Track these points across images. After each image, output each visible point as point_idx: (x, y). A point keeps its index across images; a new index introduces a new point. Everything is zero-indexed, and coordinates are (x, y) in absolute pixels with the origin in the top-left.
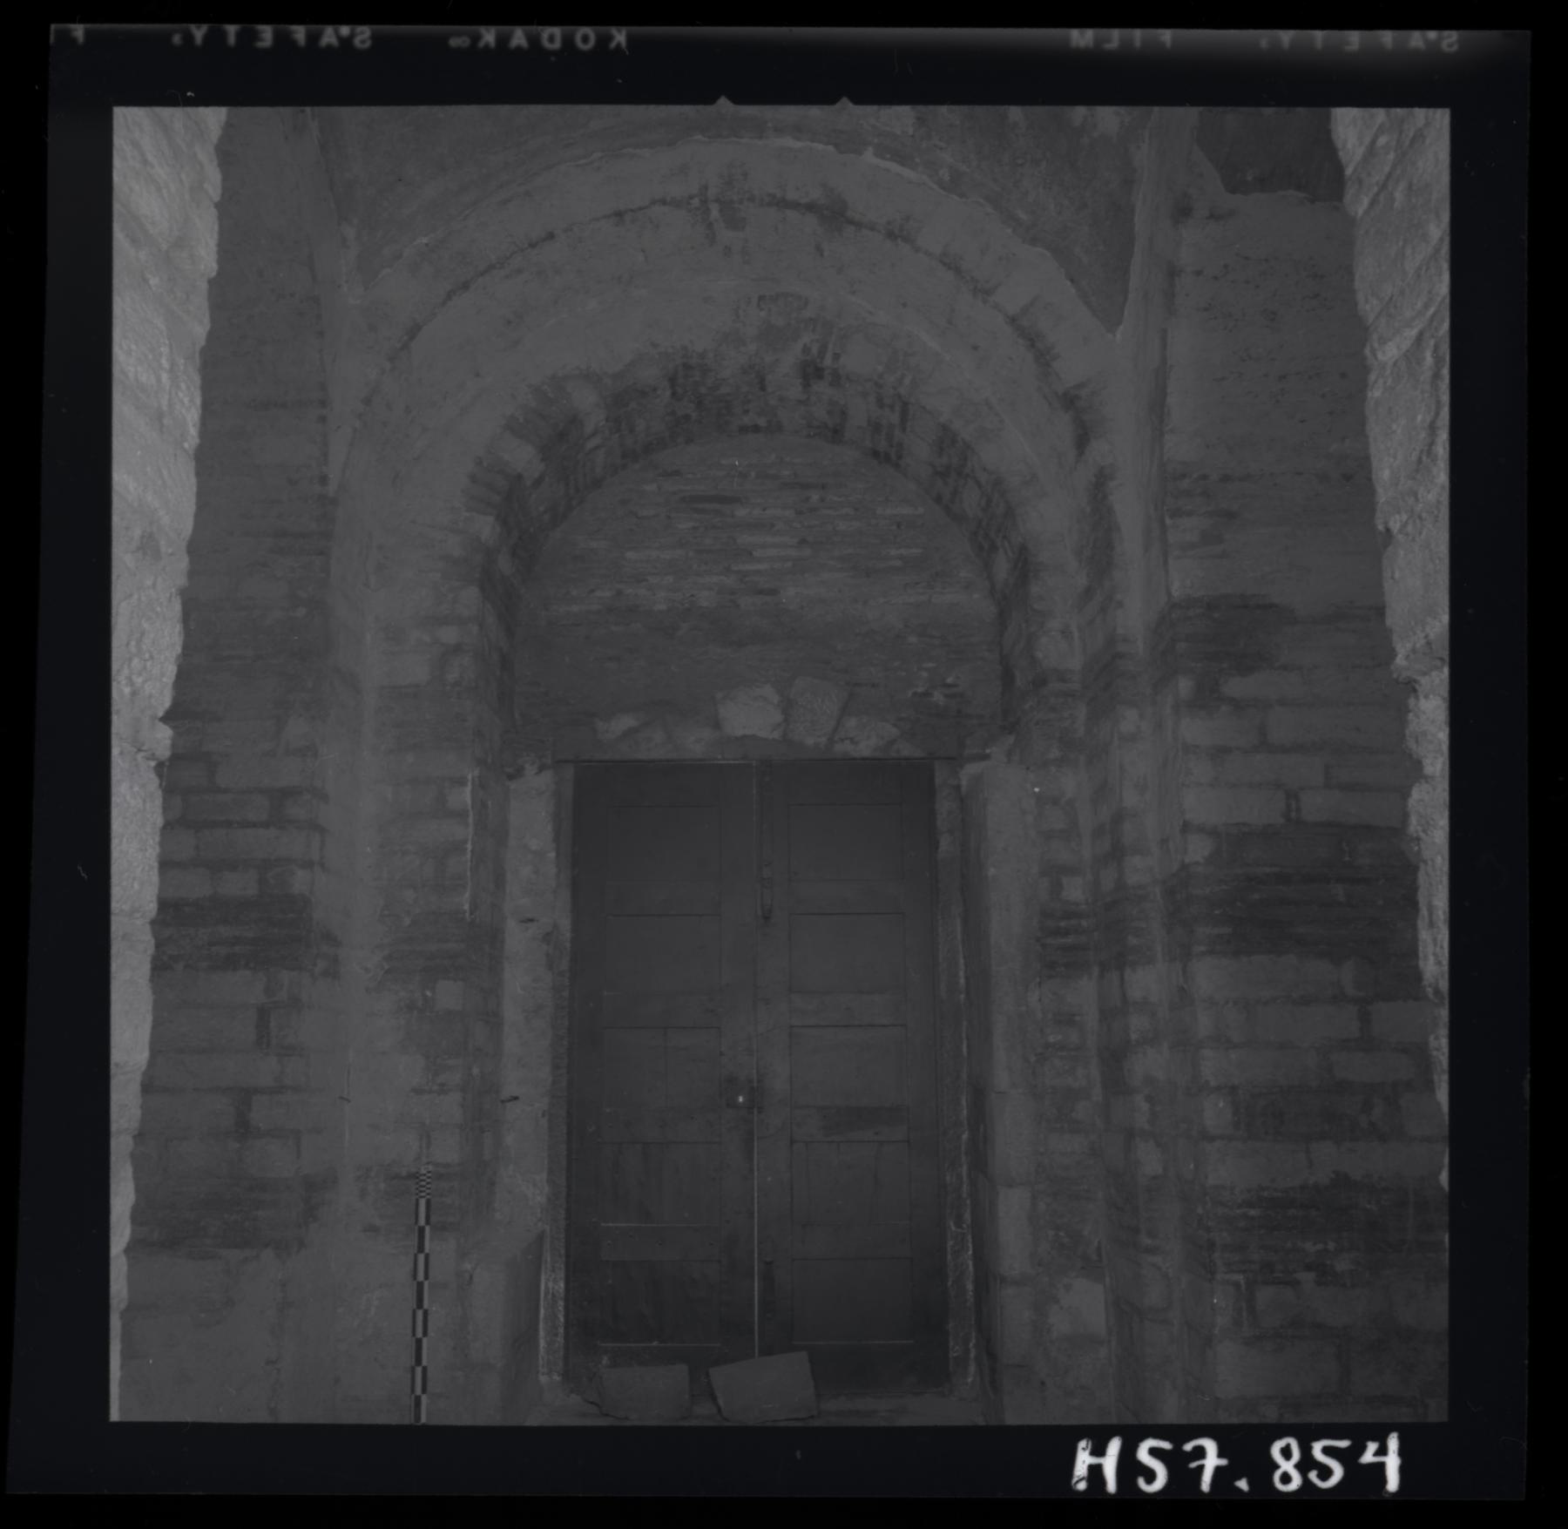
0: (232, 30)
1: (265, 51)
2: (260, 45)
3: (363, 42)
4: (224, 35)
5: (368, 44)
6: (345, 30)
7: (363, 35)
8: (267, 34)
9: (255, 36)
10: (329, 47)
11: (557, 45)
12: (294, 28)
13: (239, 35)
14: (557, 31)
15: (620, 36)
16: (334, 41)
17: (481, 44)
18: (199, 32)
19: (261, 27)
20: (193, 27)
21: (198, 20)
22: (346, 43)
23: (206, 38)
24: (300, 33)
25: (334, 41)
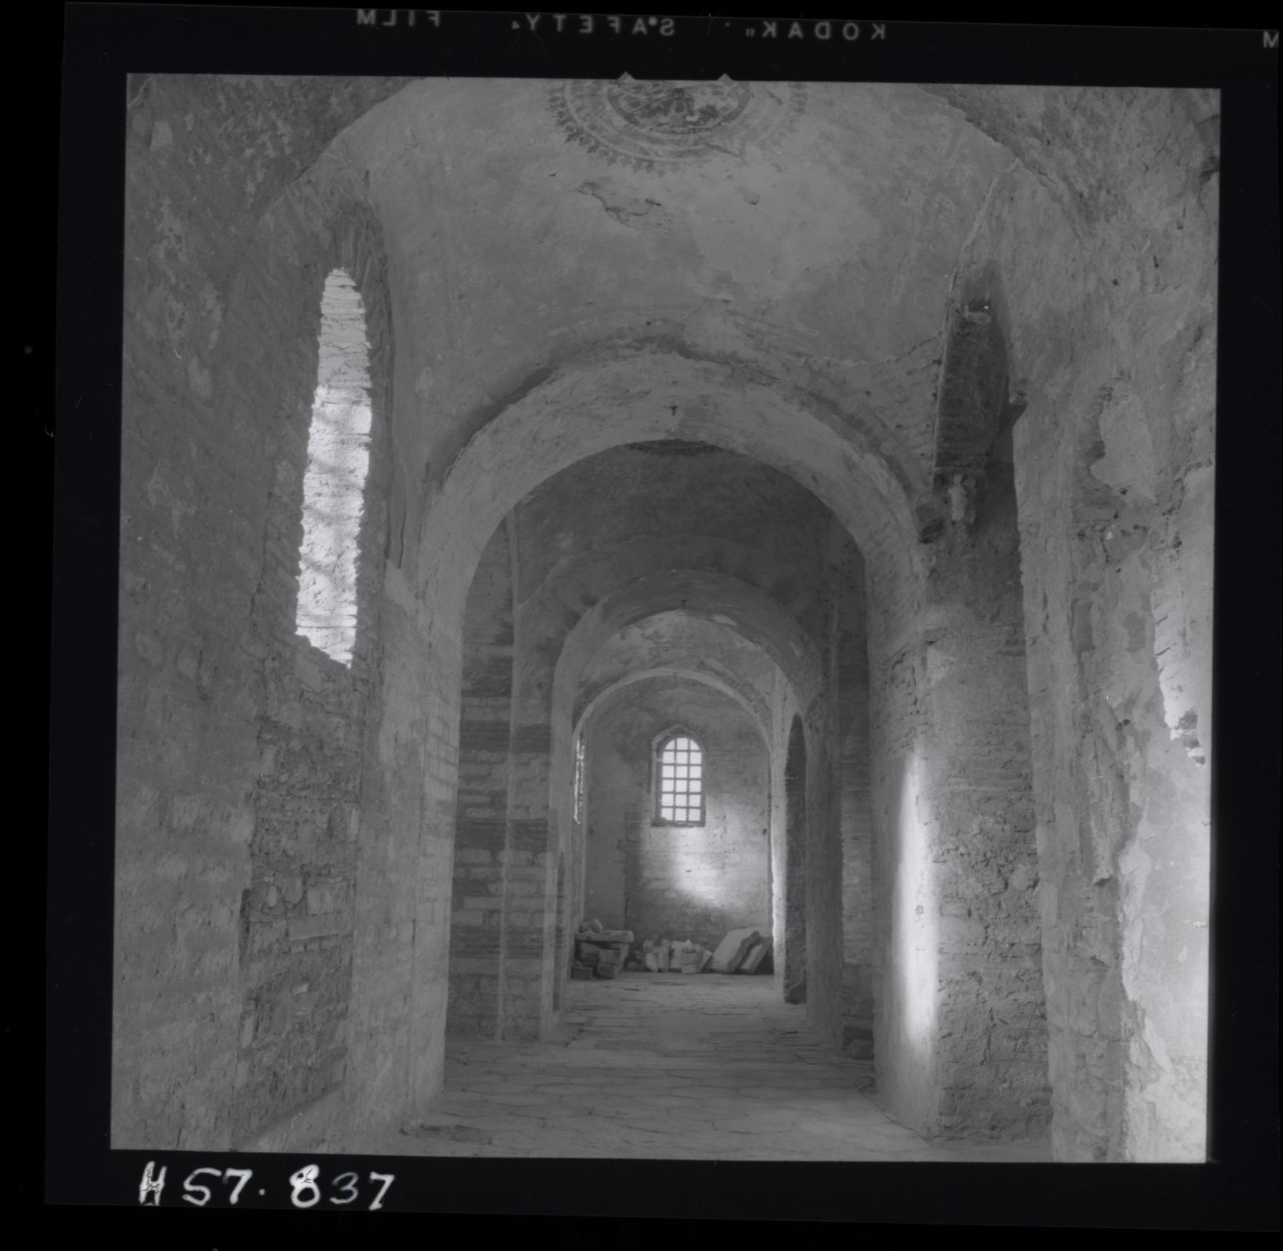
0: (560, 18)
1: (585, 35)
2: (583, 31)
3: (667, 30)
4: (555, 21)
5: (671, 32)
6: (653, 21)
7: (668, 26)
8: (589, 23)
9: (580, 24)
10: (640, 33)
11: (827, 36)
12: (611, 18)
13: (565, 23)
14: (827, 24)
15: (880, 31)
16: (643, 29)
17: (765, 34)
18: (533, 21)
19: (583, 17)
20: (528, 17)
21: (533, 10)
22: (654, 30)
23: (539, 24)
24: (616, 23)
25: (643, 29)
